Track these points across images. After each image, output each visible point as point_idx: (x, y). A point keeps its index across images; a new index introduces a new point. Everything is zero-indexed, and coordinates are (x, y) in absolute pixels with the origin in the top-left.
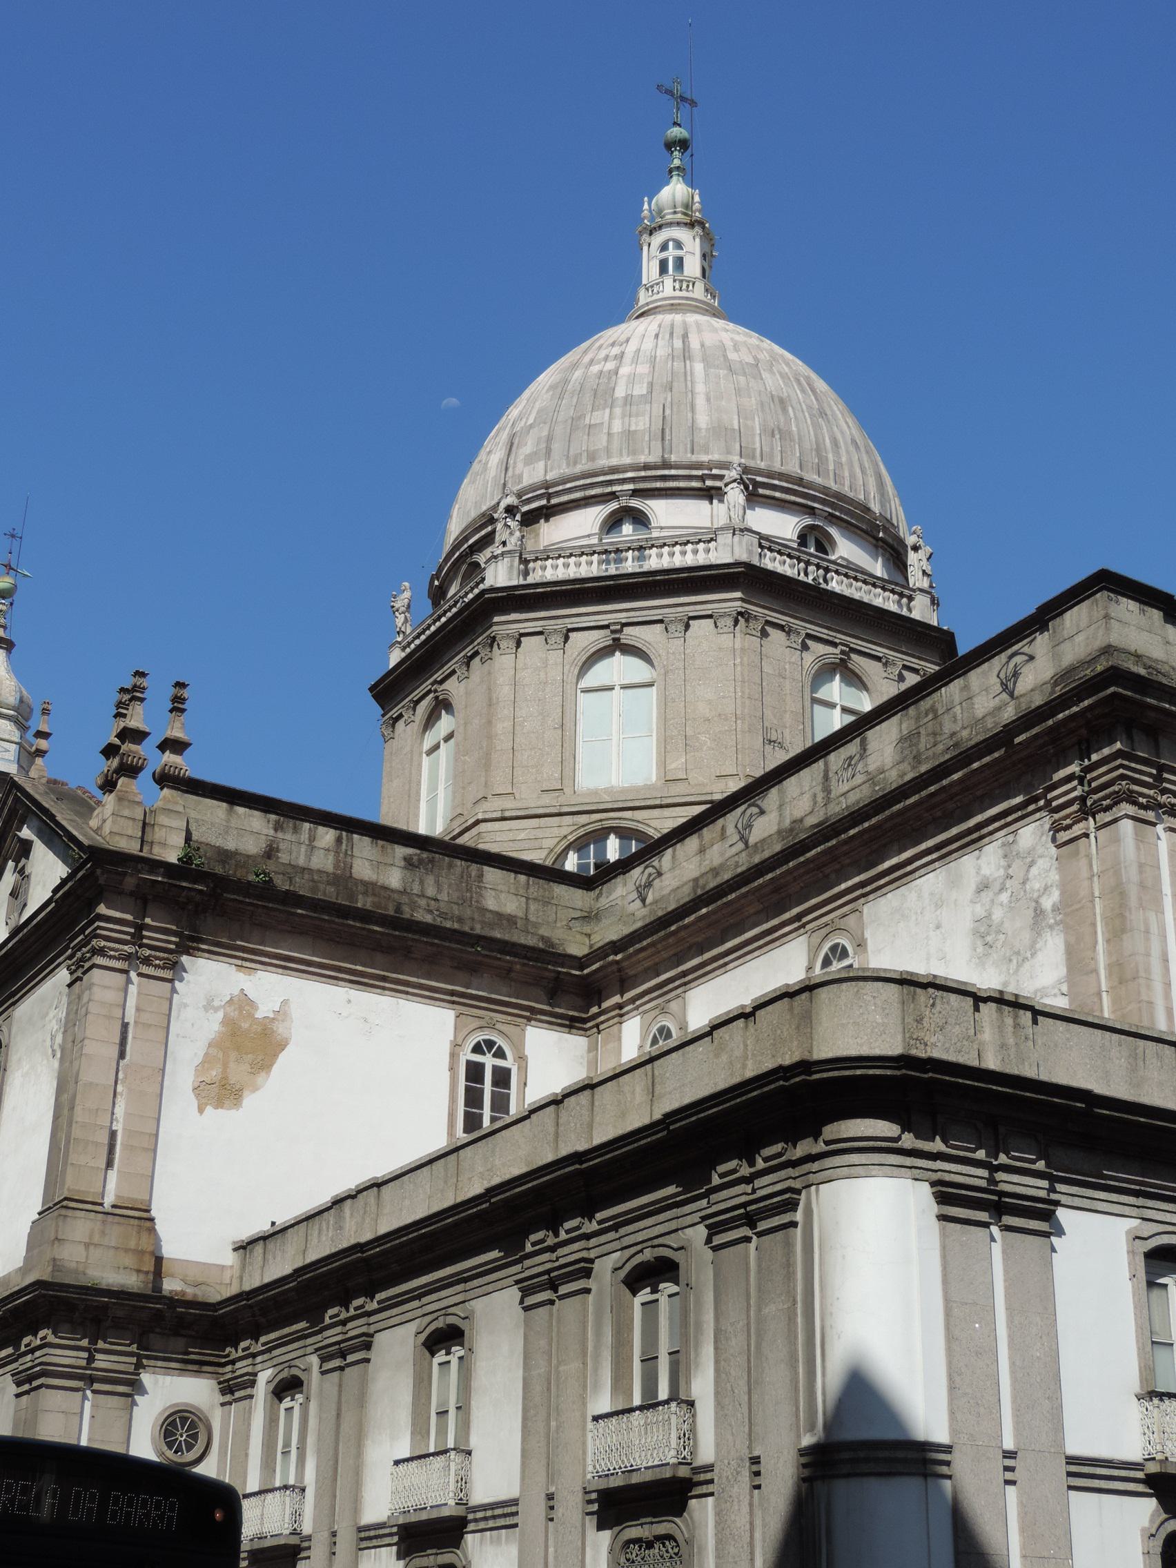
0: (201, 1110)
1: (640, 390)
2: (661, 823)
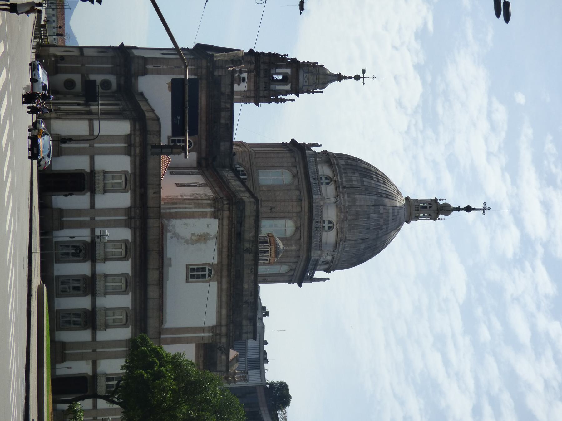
1: (365, 183)
2: (249, 185)
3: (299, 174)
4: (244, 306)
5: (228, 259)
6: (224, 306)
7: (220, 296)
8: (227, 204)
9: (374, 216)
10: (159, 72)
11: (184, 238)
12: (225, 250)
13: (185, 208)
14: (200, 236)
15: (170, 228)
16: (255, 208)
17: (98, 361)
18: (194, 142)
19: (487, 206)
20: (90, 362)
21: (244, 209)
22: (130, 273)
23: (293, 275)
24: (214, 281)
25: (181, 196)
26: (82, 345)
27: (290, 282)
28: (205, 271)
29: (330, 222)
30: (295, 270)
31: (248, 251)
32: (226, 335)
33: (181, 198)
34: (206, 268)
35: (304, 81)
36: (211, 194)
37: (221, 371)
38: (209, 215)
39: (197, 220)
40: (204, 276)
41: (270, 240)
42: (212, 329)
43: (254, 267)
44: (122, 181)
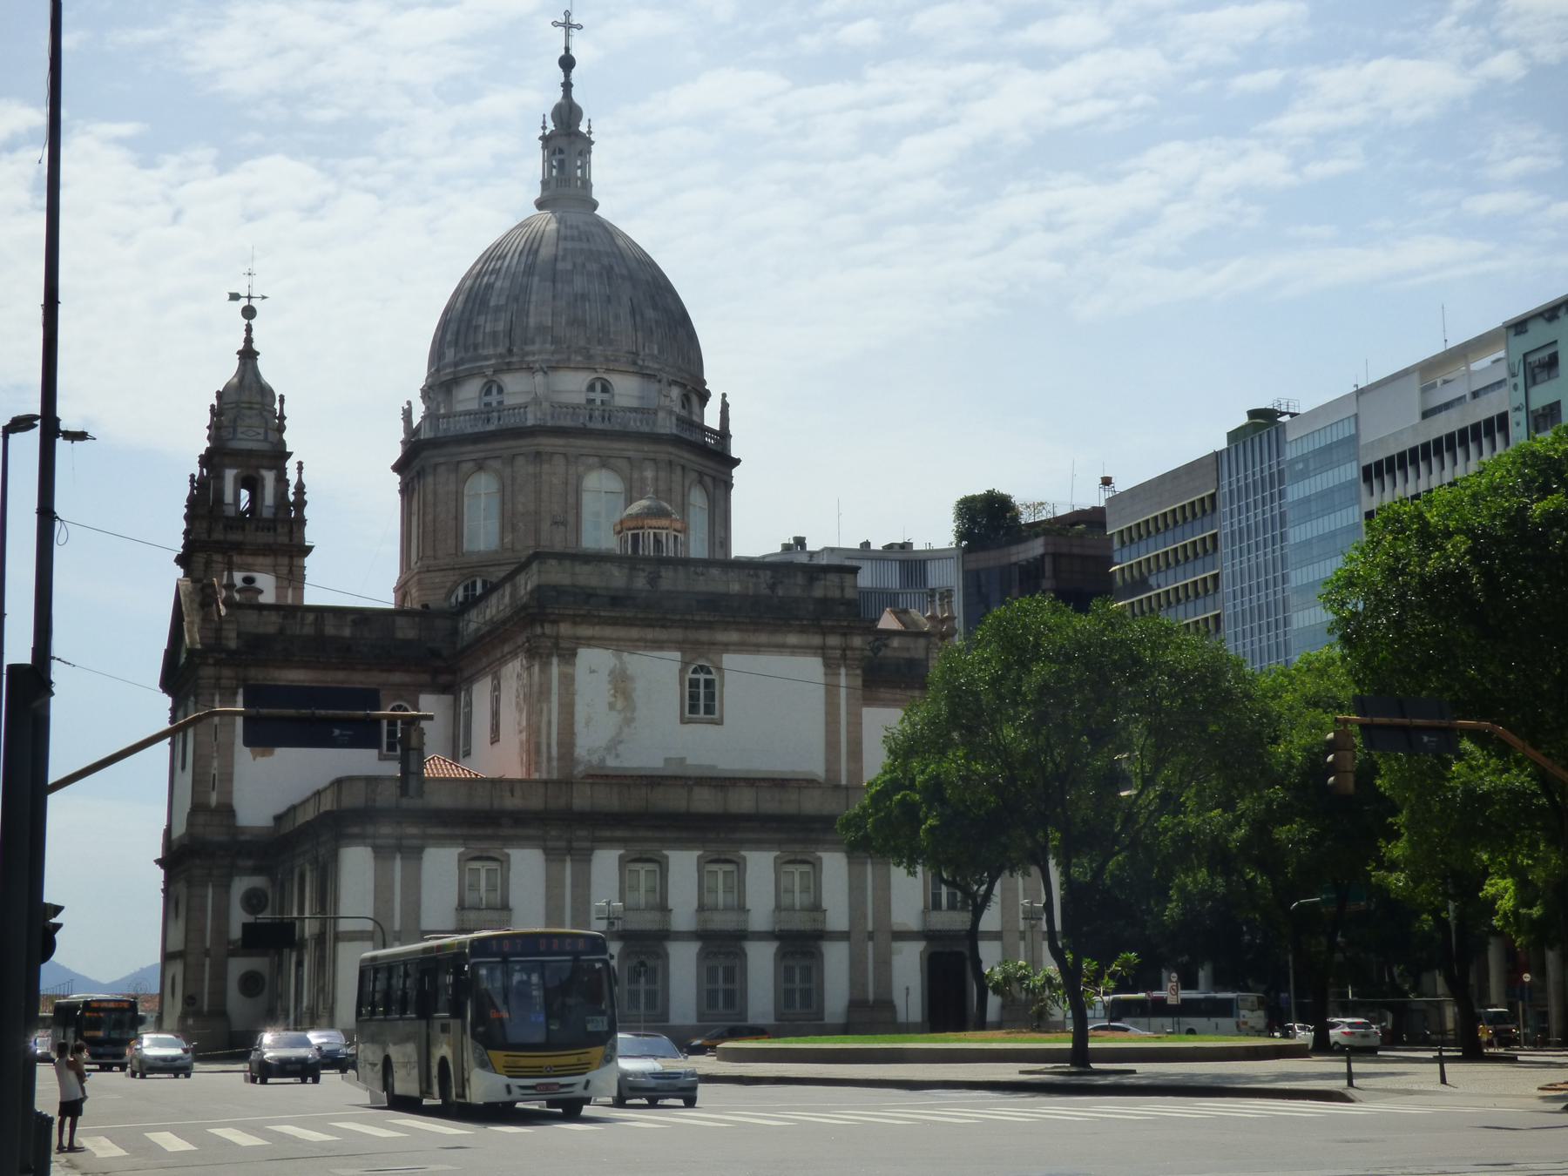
0: (254, 759)
1: (502, 301)
3: (474, 456)
4: (780, 592)
5: (671, 627)
6: (778, 638)
7: (757, 648)
8: (543, 627)
9: (579, 284)
10: (228, 777)
11: (621, 728)
12: (650, 634)
13: (549, 723)
14: (616, 692)
15: (595, 759)
16: (554, 562)
17: (895, 928)
18: (395, 700)
19: (562, 19)
20: (897, 945)
21: (555, 588)
22: (696, 853)
23: (714, 479)
24: (721, 661)
25: (521, 732)
26: (856, 964)
27: (728, 485)
28: (698, 680)
29: (591, 388)
30: (701, 474)
31: (654, 580)
32: (844, 635)
33: (524, 734)
34: (690, 680)
35: (254, 438)
36: (519, 664)
37: (927, 649)
38: (568, 670)
39: (578, 699)
40: (709, 684)
41: (630, 529)
42: (830, 666)
43: (692, 569)
44: (483, 867)
